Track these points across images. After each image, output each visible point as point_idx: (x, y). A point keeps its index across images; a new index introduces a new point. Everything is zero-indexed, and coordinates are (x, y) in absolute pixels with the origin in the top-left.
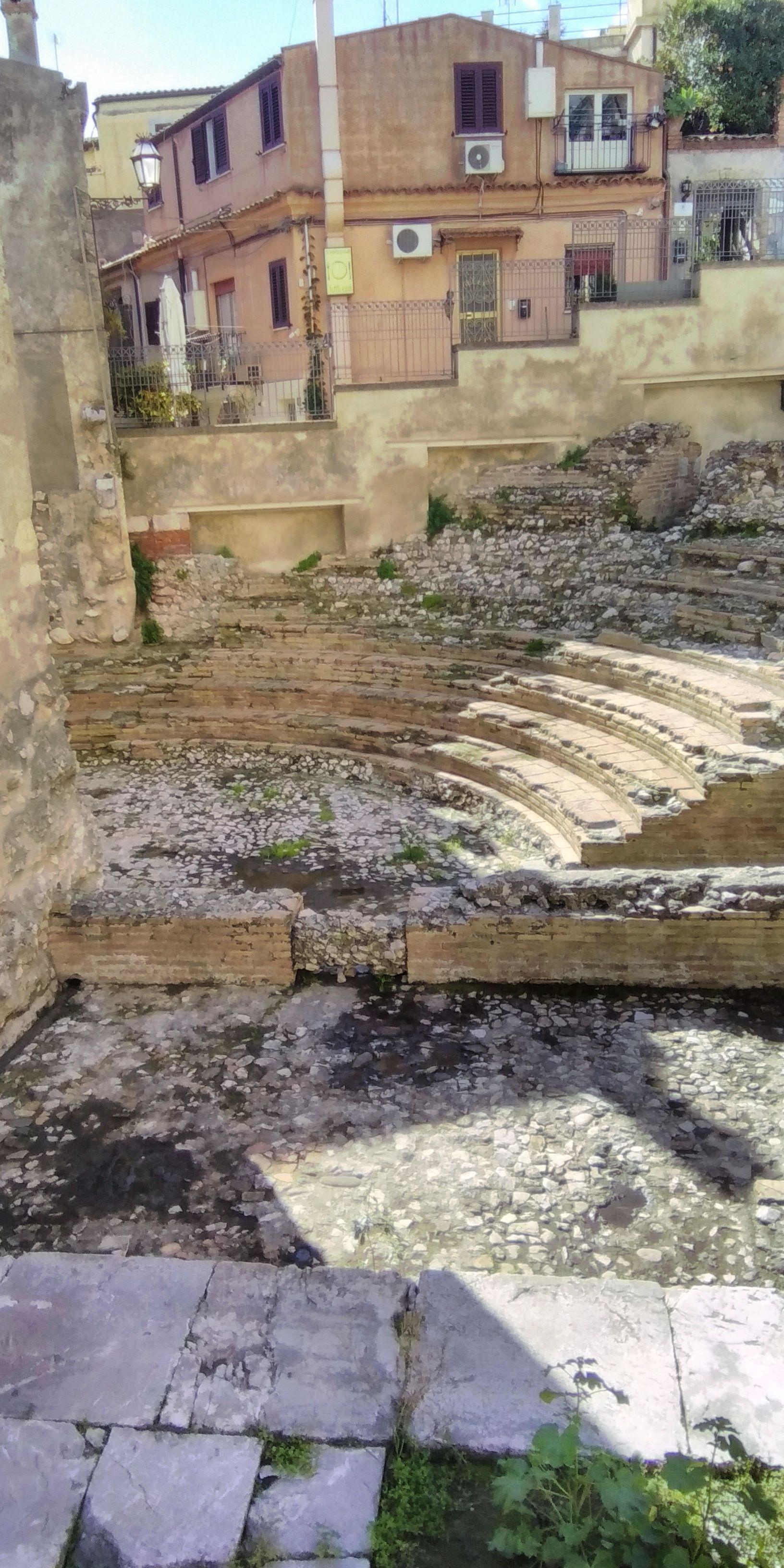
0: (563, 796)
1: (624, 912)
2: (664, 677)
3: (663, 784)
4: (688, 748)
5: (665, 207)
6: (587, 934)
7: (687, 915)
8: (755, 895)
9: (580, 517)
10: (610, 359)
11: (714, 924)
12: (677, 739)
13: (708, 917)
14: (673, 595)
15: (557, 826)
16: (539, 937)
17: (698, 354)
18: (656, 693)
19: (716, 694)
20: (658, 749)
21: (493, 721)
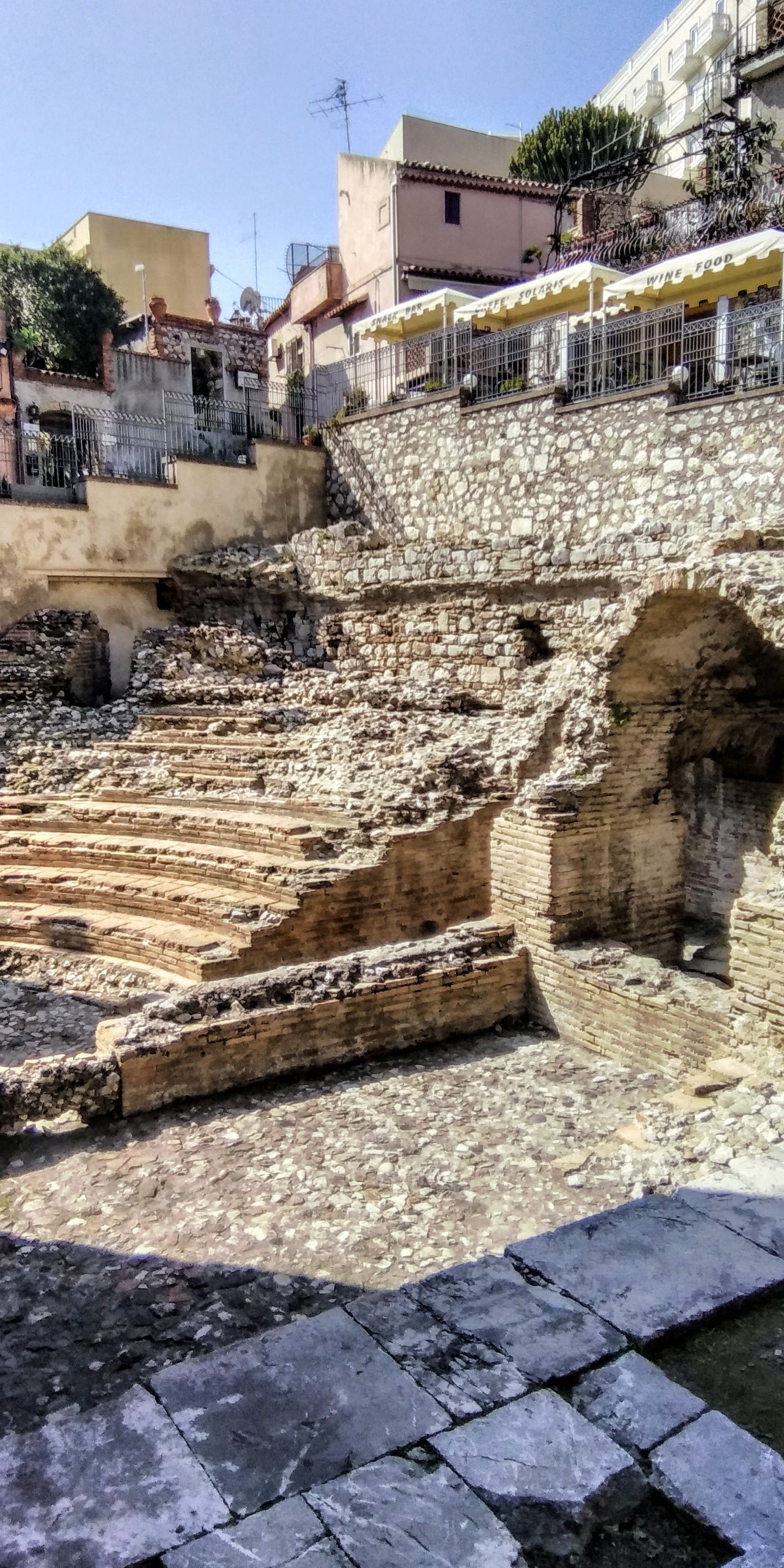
0: (147, 932)
1: (308, 999)
2: (194, 819)
3: (252, 903)
4: (262, 869)
5: (17, 424)
6: (284, 1026)
7: (360, 990)
8: (401, 966)
9: (19, 692)
10: (16, 551)
11: (380, 995)
12: (241, 865)
13: (375, 990)
14: (155, 754)
15: (151, 961)
16: (246, 1039)
17: (92, 554)
18: (189, 834)
19: (259, 825)
20: (223, 878)
21: (18, 881)
